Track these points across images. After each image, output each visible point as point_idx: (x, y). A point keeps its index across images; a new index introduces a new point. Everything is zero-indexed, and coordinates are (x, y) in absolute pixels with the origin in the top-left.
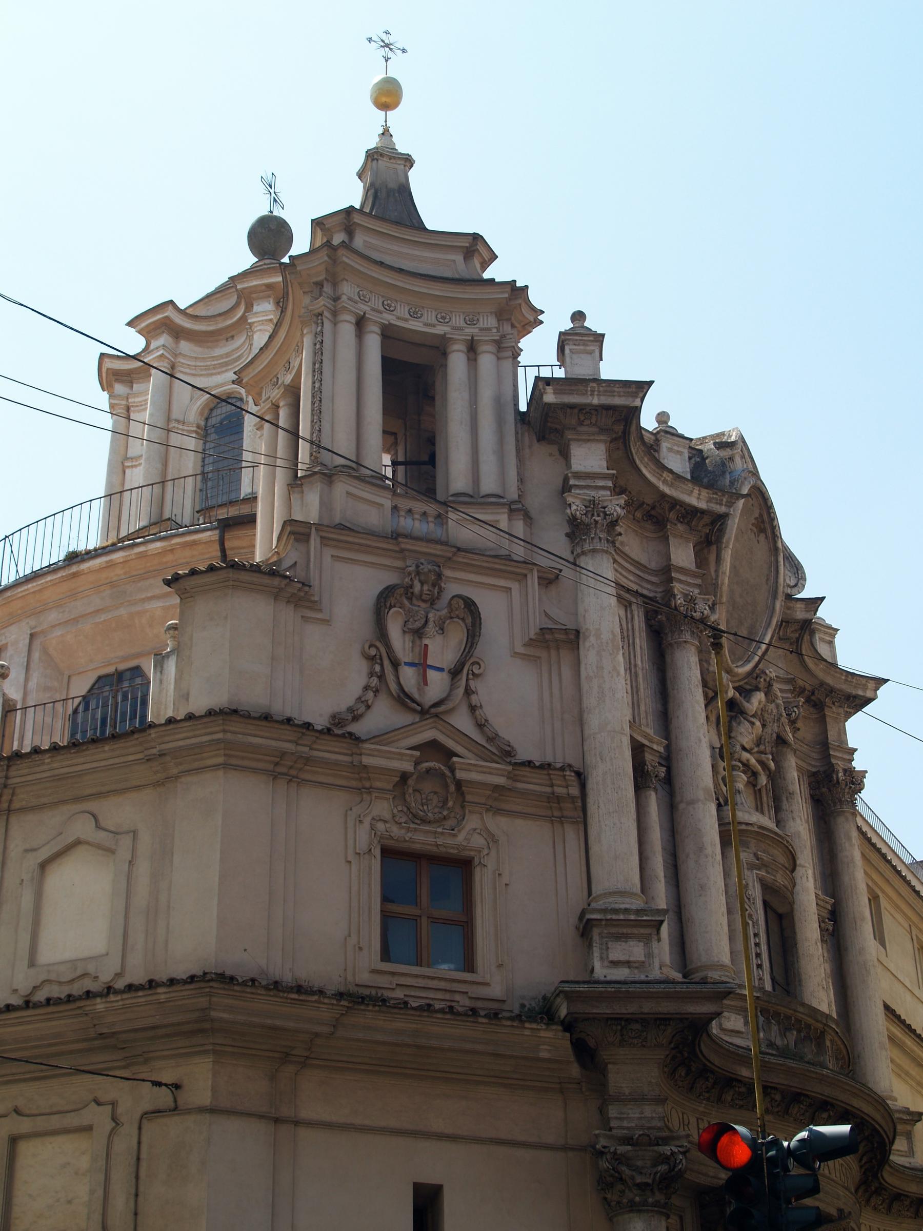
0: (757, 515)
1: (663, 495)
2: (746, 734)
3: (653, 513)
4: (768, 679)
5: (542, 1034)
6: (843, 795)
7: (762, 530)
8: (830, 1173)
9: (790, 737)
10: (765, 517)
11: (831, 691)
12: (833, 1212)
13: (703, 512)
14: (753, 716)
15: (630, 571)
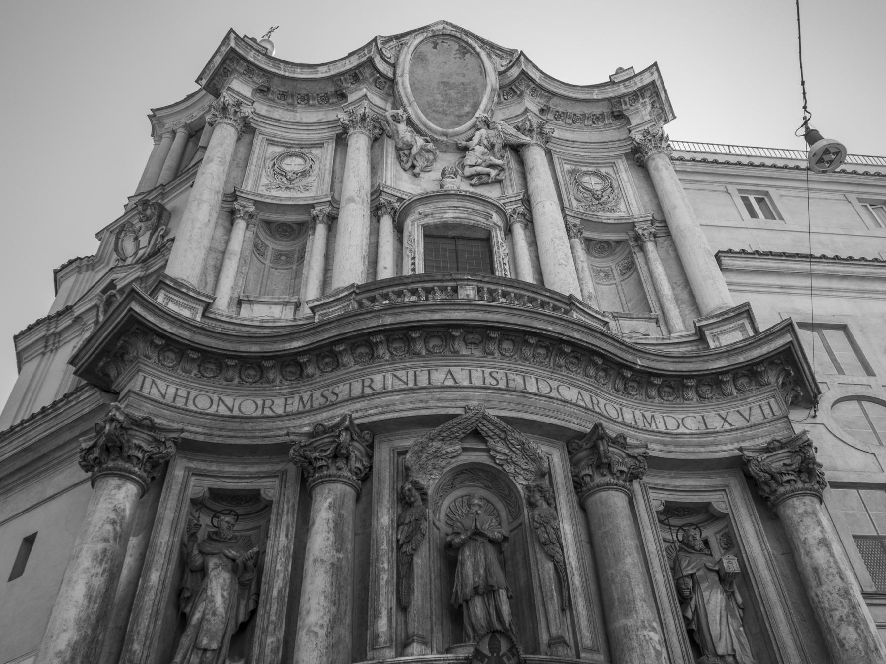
0: (457, 47)
1: (331, 77)
2: (470, 159)
3: (338, 93)
4: (480, 120)
5: (82, 398)
6: (648, 148)
7: (468, 51)
8: (456, 382)
9: (525, 139)
10: (464, 45)
11: (619, 99)
12: (459, 411)
13: (359, 66)
14: (479, 144)
15: (323, 129)
